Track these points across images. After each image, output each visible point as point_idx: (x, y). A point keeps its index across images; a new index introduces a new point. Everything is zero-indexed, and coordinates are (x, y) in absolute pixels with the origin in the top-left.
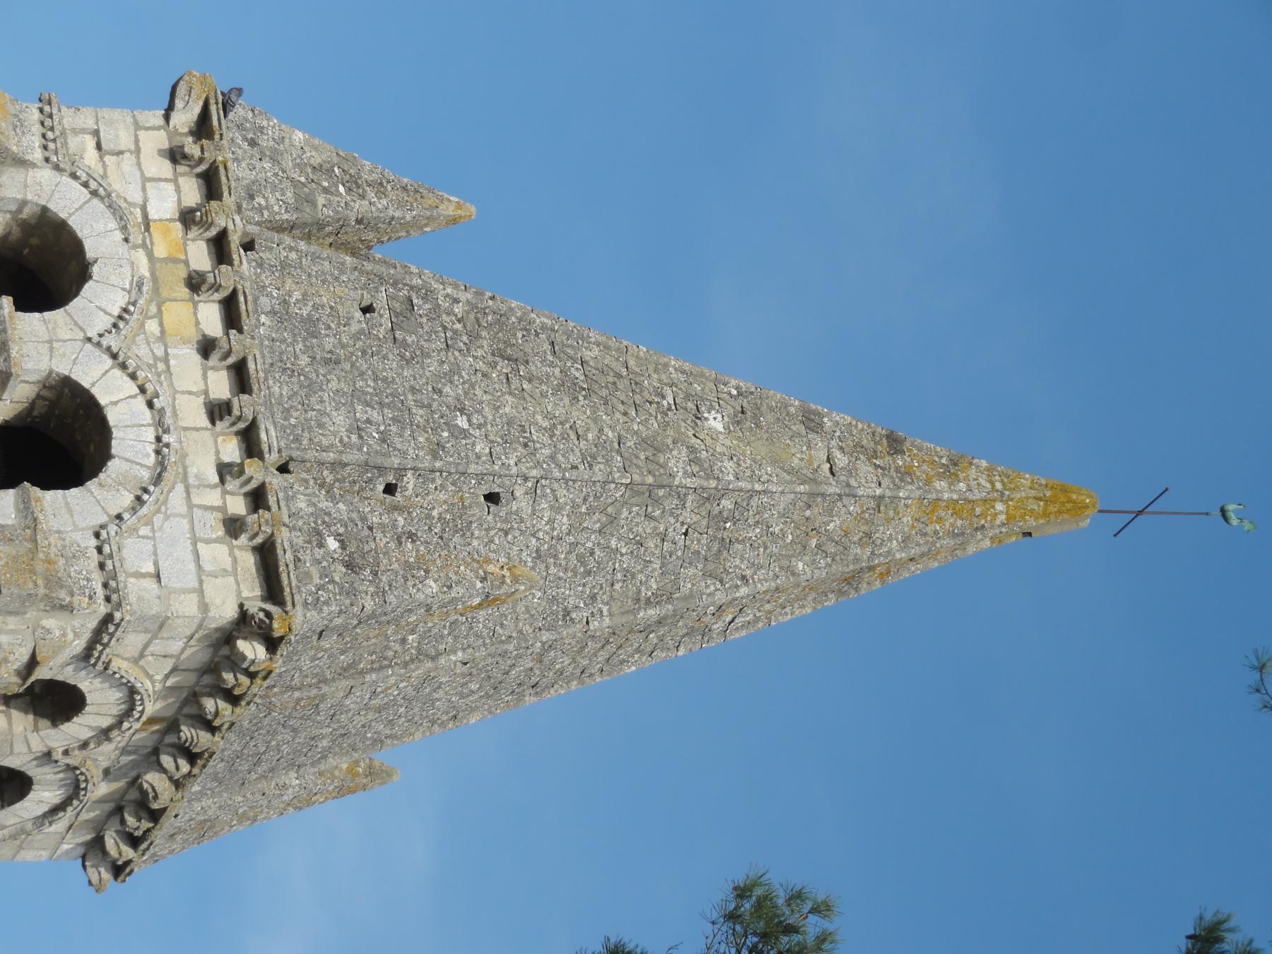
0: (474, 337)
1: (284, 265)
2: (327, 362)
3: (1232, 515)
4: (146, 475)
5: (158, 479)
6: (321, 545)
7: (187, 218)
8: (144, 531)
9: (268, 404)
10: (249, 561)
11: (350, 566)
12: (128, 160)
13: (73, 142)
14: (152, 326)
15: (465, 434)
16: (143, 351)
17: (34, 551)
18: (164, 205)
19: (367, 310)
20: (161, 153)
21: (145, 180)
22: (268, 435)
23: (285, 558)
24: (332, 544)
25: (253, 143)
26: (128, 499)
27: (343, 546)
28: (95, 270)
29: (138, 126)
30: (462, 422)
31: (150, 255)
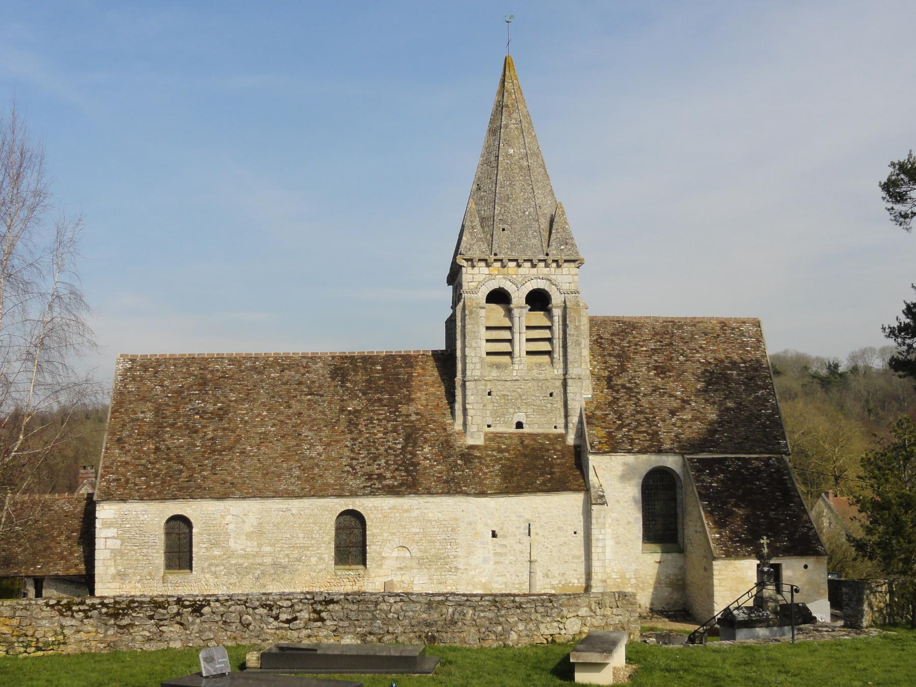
0: (505, 206)
1: (499, 247)
2: (520, 241)
3: (509, 20)
4: (548, 282)
5: (551, 281)
6: (563, 250)
7: (488, 265)
8: (560, 284)
9: (535, 256)
10: (566, 264)
11: (567, 244)
12: (474, 276)
13: (471, 287)
14: (514, 276)
15: (529, 213)
16: (520, 279)
17: (573, 308)
18: (486, 270)
19: (503, 230)
20: (473, 269)
21: (479, 273)
22: (542, 257)
23: (568, 258)
24: (562, 247)
25: (470, 249)
26: (553, 287)
27: (562, 245)
28: (501, 286)
29: (467, 273)
30: (527, 213)
31: (497, 275)
